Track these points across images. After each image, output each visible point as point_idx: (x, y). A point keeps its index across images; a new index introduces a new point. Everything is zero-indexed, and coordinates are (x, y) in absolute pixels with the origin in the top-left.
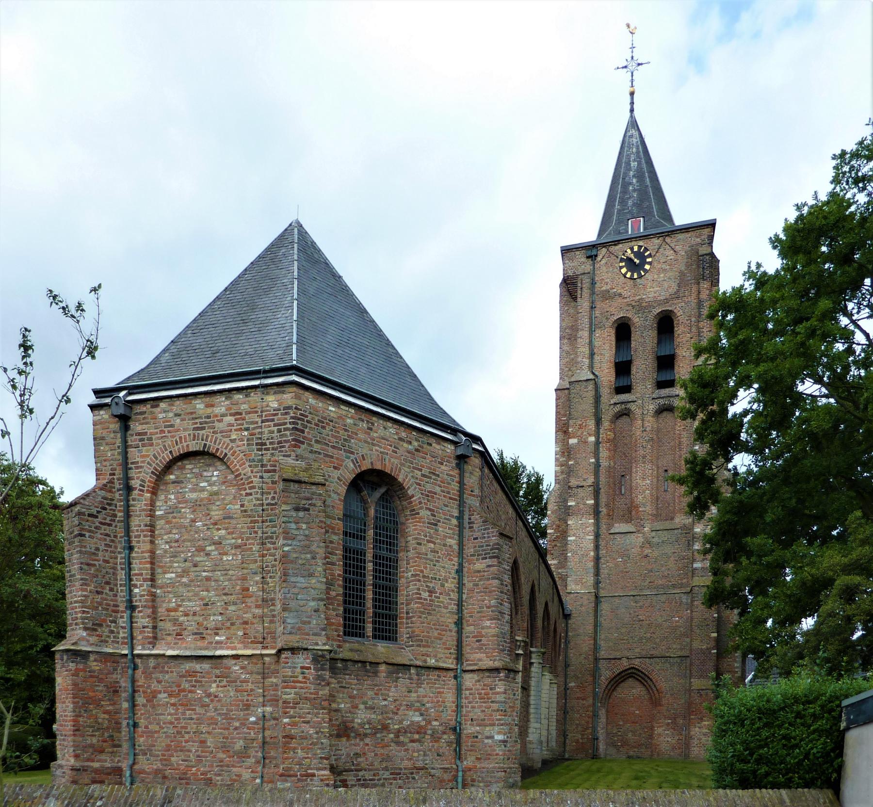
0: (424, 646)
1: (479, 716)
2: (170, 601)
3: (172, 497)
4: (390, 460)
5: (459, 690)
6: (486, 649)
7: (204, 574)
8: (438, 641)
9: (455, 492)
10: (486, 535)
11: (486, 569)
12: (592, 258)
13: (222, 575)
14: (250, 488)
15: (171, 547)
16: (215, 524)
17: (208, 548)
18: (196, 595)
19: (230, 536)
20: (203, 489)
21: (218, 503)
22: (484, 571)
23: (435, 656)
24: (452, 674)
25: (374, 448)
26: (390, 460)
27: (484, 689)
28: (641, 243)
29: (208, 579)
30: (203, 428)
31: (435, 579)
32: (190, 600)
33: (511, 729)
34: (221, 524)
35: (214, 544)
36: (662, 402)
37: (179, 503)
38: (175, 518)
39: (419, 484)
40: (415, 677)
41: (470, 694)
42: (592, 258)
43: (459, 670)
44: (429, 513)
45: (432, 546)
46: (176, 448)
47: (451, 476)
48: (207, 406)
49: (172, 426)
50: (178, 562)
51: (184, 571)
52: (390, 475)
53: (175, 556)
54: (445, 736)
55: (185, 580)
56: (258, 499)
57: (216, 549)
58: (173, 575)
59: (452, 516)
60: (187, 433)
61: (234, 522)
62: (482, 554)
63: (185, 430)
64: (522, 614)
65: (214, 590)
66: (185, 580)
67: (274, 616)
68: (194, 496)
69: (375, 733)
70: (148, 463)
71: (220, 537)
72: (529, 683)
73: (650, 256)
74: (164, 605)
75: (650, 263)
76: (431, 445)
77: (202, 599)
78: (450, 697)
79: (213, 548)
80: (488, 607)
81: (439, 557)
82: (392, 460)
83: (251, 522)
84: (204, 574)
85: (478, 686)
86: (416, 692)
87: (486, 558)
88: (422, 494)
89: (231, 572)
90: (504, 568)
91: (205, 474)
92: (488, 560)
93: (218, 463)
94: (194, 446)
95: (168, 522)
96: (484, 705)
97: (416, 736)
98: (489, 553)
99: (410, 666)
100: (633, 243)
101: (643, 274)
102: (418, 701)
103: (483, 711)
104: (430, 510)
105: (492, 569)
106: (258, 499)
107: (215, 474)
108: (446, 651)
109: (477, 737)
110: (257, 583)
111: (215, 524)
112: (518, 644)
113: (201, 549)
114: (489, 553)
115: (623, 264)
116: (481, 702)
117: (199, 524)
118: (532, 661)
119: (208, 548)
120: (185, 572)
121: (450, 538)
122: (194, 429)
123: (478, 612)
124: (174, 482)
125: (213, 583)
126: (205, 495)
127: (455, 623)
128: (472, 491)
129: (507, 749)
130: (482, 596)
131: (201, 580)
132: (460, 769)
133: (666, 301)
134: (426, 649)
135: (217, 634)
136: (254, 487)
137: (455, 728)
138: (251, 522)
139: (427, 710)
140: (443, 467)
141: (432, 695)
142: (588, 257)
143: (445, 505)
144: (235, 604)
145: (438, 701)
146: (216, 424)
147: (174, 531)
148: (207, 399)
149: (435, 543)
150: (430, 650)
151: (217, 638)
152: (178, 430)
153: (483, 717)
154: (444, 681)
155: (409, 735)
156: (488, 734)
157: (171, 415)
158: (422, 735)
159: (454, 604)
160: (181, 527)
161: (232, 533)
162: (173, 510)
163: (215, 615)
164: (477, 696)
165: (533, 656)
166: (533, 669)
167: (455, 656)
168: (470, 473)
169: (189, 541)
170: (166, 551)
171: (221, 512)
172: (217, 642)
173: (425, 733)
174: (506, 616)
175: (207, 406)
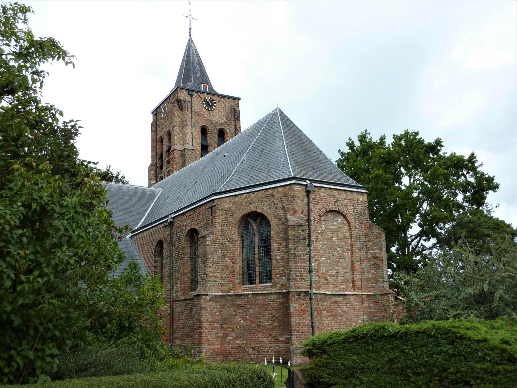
2: (323, 270)
13: (343, 261)
15: (323, 247)
16: (340, 240)
17: (338, 249)
19: (345, 245)
20: (335, 225)
21: (341, 232)
29: (338, 262)
32: (331, 270)
34: (342, 240)
35: (340, 247)
46: (328, 208)
49: (326, 199)
50: (326, 253)
51: (328, 257)
53: (325, 251)
55: (329, 261)
57: (341, 250)
58: (324, 259)
60: (332, 203)
61: (347, 240)
63: (331, 201)
65: (340, 266)
66: (329, 261)
68: (332, 227)
70: (317, 211)
71: (342, 245)
73: (215, 103)
74: (321, 271)
75: (215, 106)
77: (336, 270)
84: (337, 259)
91: (336, 219)
93: (341, 216)
94: (335, 209)
107: (340, 219)
111: (340, 240)
113: (335, 249)
119: (338, 249)
120: (329, 258)
122: (334, 202)
125: (340, 264)
126: (336, 227)
131: (335, 262)
133: (222, 124)
157: (326, 194)
160: (327, 239)
161: (346, 244)
162: (324, 231)
169: (330, 245)
170: (321, 248)
171: (342, 235)
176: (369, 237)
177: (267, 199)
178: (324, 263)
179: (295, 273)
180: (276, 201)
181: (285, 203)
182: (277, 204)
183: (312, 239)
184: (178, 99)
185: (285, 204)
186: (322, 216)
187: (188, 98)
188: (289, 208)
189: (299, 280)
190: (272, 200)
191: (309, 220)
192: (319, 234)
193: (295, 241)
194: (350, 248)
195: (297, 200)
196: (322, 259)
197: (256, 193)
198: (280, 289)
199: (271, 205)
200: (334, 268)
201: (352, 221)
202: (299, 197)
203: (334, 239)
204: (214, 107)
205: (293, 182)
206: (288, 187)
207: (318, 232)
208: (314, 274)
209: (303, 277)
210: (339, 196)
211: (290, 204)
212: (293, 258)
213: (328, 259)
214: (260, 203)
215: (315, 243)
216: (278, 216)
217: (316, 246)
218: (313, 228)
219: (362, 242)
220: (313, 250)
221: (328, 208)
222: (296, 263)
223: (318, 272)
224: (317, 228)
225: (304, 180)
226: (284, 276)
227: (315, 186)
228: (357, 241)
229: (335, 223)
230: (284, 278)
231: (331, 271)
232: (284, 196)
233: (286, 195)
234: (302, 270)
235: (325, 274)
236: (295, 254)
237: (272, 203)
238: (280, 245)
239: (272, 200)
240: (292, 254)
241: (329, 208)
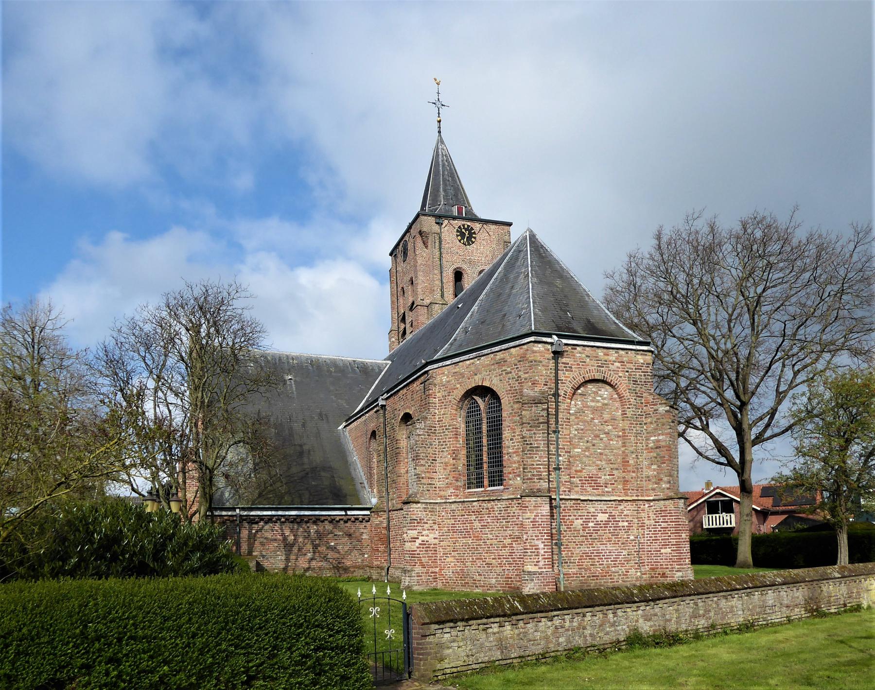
2: (577, 466)
3: (579, 403)
7: (599, 451)
14: (630, 405)
17: (601, 436)
18: (594, 463)
20: (598, 401)
28: (469, 224)
29: (601, 454)
30: (603, 367)
32: (590, 466)
37: (584, 407)
38: (581, 415)
46: (587, 375)
48: (605, 355)
49: (584, 362)
51: (586, 448)
53: (581, 439)
55: (587, 453)
56: (633, 411)
58: (580, 450)
60: (593, 368)
61: (616, 422)
63: (592, 366)
65: (605, 460)
66: (587, 453)
67: (642, 478)
68: (593, 404)
74: (574, 468)
77: (597, 466)
79: (604, 436)
83: (630, 424)
84: (599, 451)
89: (615, 451)
91: (600, 392)
93: (608, 387)
94: (598, 376)
95: (576, 418)
100: (465, 223)
106: (633, 411)
107: (605, 392)
110: (633, 458)
111: (606, 422)
113: (597, 436)
117: (596, 421)
119: (601, 436)
120: (588, 448)
124: (580, 395)
125: (604, 457)
126: (599, 404)
135: (606, 487)
136: (631, 404)
138: (630, 424)
144: (617, 469)
146: (610, 365)
147: (581, 424)
148: (605, 350)
151: (606, 489)
152: (588, 365)
157: (584, 356)
160: (585, 421)
162: (580, 411)
163: (605, 475)
169: (590, 430)
170: (575, 435)
172: (607, 492)
175: (605, 355)
176: (651, 417)
177: (496, 366)
178: (579, 456)
179: (531, 472)
180: (509, 369)
181: (520, 371)
182: (511, 373)
183: (560, 423)
184: (420, 231)
185: (520, 373)
186: (578, 388)
187: (436, 228)
188: (526, 379)
189: (536, 480)
190: (504, 368)
191: (556, 395)
192: (573, 414)
193: (531, 427)
194: (621, 433)
195: (539, 365)
196: (576, 450)
197: (482, 358)
198: (513, 494)
199: (502, 374)
200: (594, 463)
201: (627, 394)
202: (541, 362)
203: (596, 421)
205: (532, 339)
206: (525, 347)
207: (571, 412)
208: (562, 472)
209: (542, 477)
210: (606, 357)
211: (528, 373)
212: (528, 450)
213: (585, 451)
214: (488, 373)
215: (566, 428)
216: (511, 390)
217: (566, 432)
218: (562, 407)
219: (640, 424)
220: (562, 438)
221: (587, 375)
222: (533, 457)
223: (570, 469)
224: (571, 407)
225: (549, 335)
226: (519, 476)
227: (566, 344)
228: (632, 424)
229: (598, 398)
230: (519, 479)
231: (591, 468)
232: (519, 361)
233: (523, 358)
234: (541, 467)
235: (580, 471)
236: (531, 444)
237: (504, 373)
238: (514, 433)
239: (504, 368)
240: (527, 444)
241: (589, 376)
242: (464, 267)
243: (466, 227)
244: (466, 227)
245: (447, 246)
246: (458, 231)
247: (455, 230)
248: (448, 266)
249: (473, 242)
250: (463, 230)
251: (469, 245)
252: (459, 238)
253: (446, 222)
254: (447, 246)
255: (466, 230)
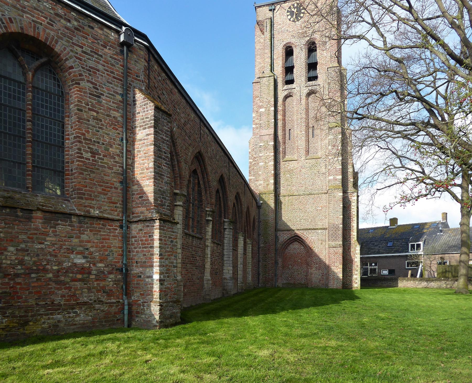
0: (87, 199)
1: (141, 259)
4: (44, 31)
5: (126, 238)
6: (146, 203)
8: (102, 196)
9: (120, 74)
10: (146, 109)
11: (146, 138)
12: (272, 10)
22: (144, 139)
23: (99, 208)
24: (118, 224)
25: (25, 15)
26: (44, 31)
27: (144, 237)
31: (98, 143)
33: (168, 270)
36: (310, 88)
39: (80, 59)
40: (76, 224)
41: (135, 241)
42: (272, 10)
43: (124, 221)
44: (91, 86)
45: (95, 114)
47: (115, 59)
52: (45, 44)
54: (112, 276)
59: (117, 93)
62: (143, 126)
64: (210, 193)
69: (30, 274)
72: (223, 241)
76: (92, 28)
78: (116, 243)
80: (147, 169)
81: (102, 125)
82: (48, 31)
85: (140, 235)
86: (79, 237)
87: (145, 128)
88: (83, 68)
90: (162, 138)
92: (147, 130)
96: (145, 250)
97: (79, 276)
98: (148, 124)
99: (71, 214)
101: (300, 18)
102: (81, 246)
103: (144, 255)
104: (92, 83)
105: (150, 137)
108: (112, 205)
109: (140, 277)
112: (208, 213)
114: (148, 124)
115: (289, 14)
116: (143, 248)
118: (225, 227)
121: (114, 110)
123: (141, 174)
127: (121, 182)
128: (137, 76)
129: (164, 287)
130: (143, 160)
132: (126, 302)
134: (90, 201)
137: (122, 269)
139: (91, 253)
140: (106, 50)
141: (96, 241)
142: (270, 10)
143: (108, 82)
145: (104, 246)
149: (98, 113)
150: (94, 202)
153: (144, 260)
154: (109, 229)
155: (71, 275)
156: (148, 275)
158: (85, 276)
159: (120, 167)
164: (140, 242)
165: (226, 224)
166: (226, 232)
167: (120, 209)
168: (136, 61)
173: (90, 273)
174: (165, 177)
187: (270, 14)
204: (302, 15)
242: (293, 41)
243: (296, 5)
244: (296, 5)
245: (279, 27)
246: (288, 12)
247: (286, 11)
248: (279, 44)
249: (302, 17)
250: (293, 10)
251: (298, 20)
252: (289, 17)
253: (278, 6)
254: (279, 27)
255: (294, 8)
